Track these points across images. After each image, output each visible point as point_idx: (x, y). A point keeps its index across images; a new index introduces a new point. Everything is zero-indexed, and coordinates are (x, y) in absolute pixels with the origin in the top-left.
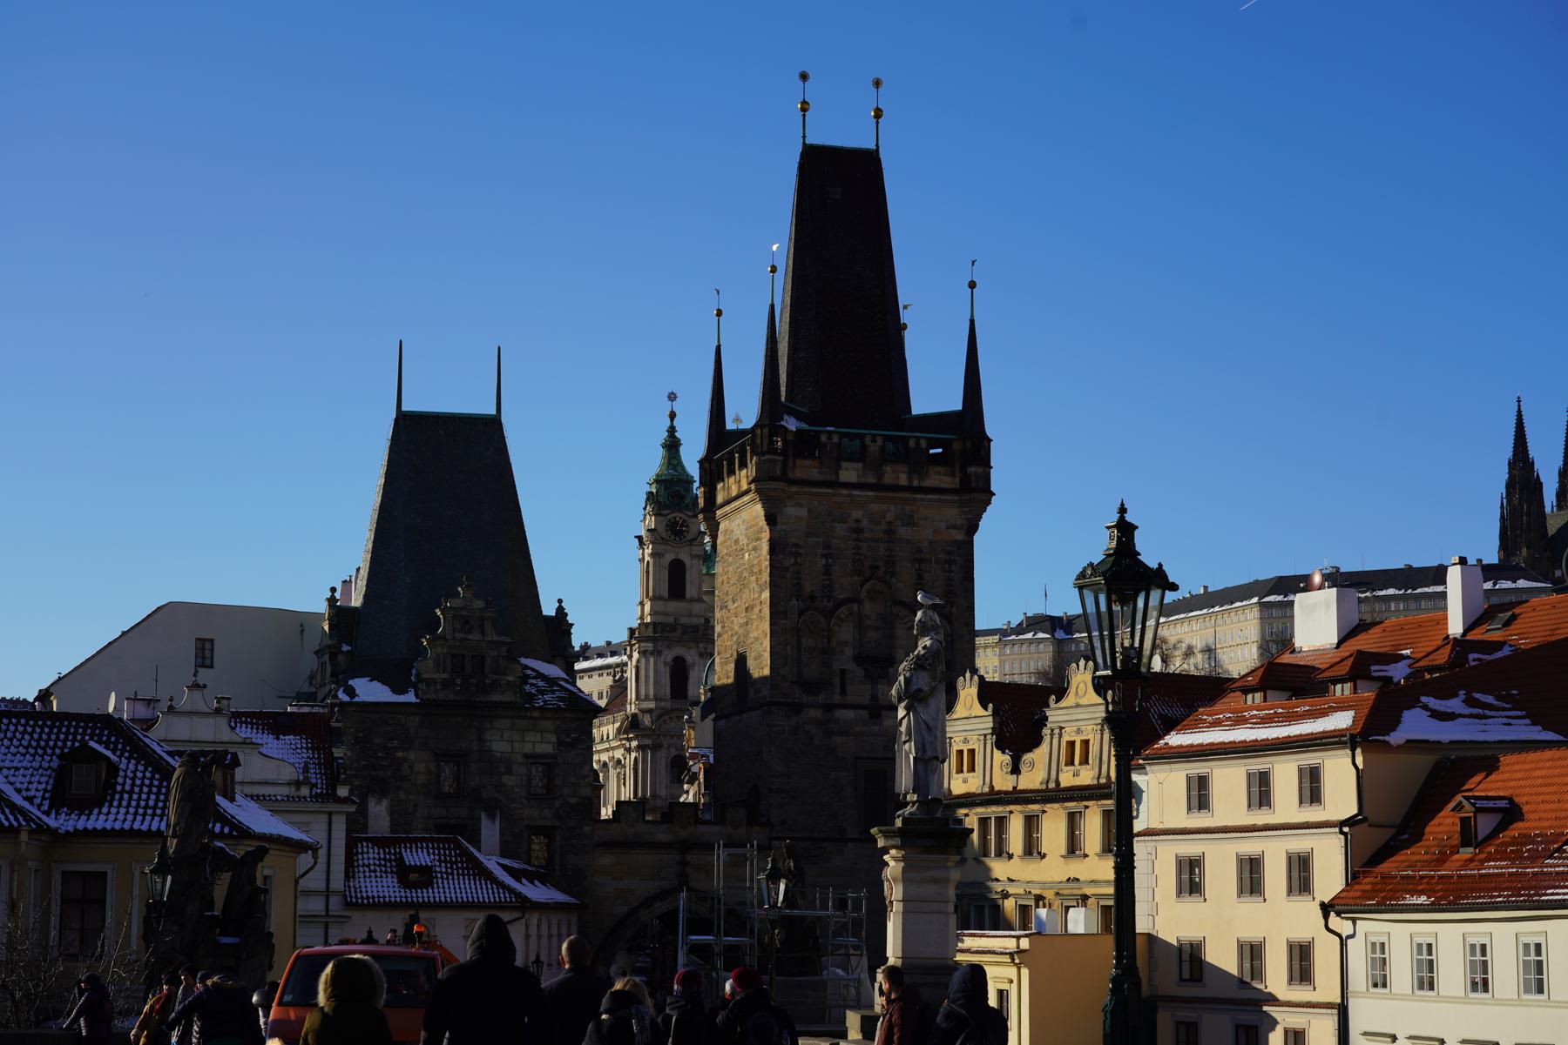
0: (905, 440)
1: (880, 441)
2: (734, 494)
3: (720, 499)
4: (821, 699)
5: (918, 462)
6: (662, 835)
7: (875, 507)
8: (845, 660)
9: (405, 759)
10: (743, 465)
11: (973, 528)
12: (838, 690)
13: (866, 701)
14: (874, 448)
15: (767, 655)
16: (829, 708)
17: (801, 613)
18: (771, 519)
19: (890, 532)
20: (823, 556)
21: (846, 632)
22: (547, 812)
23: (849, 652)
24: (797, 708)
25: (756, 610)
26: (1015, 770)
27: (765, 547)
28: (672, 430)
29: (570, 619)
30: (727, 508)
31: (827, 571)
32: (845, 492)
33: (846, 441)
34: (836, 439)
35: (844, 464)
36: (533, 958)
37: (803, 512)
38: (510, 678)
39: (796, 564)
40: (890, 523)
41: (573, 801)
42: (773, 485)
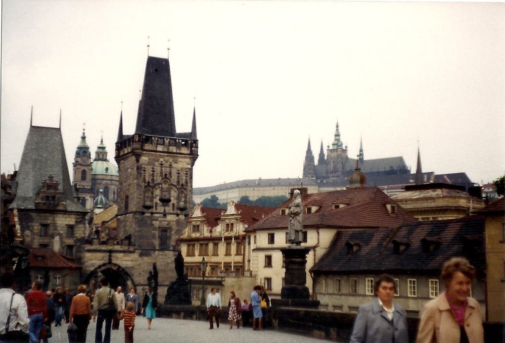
0: (176, 139)
2: (126, 152)
3: (121, 154)
4: (150, 210)
5: (177, 145)
7: (166, 158)
8: (157, 200)
9: (31, 225)
10: (129, 145)
11: (193, 165)
12: (154, 208)
13: (162, 211)
14: (167, 141)
19: (171, 166)
23: (158, 198)
24: (143, 213)
26: (211, 231)
27: (136, 168)
28: (84, 134)
32: (159, 153)
33: (159, 139)
35: (158, 146)
38: (64, 203)
40: (171, 163)
42: (138, 151)
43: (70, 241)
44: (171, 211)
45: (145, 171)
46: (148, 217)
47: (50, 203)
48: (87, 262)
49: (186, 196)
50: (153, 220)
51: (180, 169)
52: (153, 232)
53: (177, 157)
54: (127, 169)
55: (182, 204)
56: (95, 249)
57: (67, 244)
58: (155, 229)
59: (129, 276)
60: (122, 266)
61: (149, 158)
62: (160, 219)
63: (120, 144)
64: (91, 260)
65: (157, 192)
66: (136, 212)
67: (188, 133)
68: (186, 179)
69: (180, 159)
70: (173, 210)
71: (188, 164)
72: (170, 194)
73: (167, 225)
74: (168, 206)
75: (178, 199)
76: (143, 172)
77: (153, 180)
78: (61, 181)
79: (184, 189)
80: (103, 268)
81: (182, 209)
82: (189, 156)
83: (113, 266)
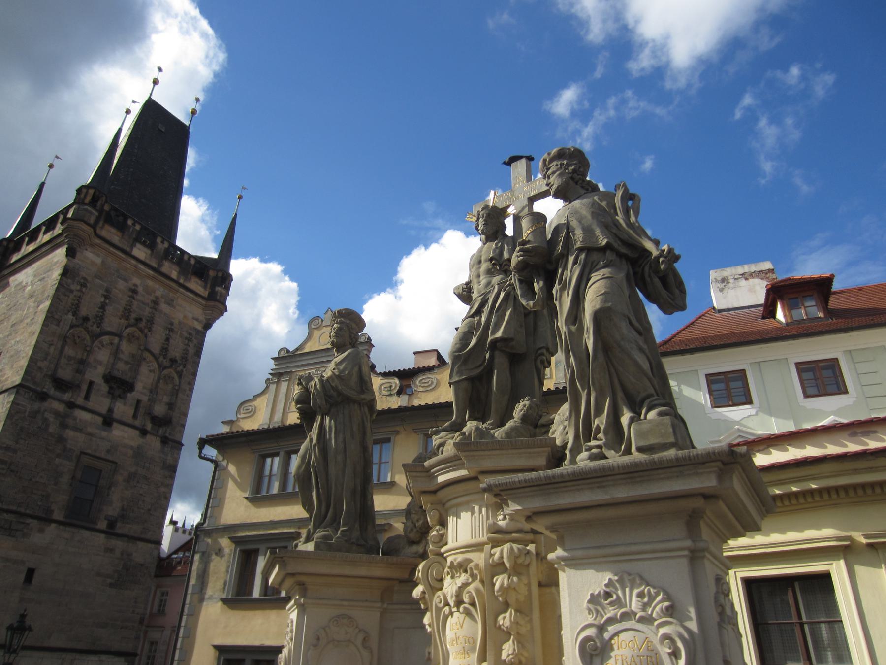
1: (166, 245)
4: (67, 396)
7: (150, 283)
8: (96, 374)
11: (208, 326)
12: (83, 394)
13: (104, 410)
14: (162, 246)
16: (71, 405)
17: (72, 327)
18: (71, 253)
19: (156, 303)
20: (103, 295)
21: (103, 355)
23: (101, 370)
24: (43, 397)
25: (28, 320)
30: (18, 265)
31: (103, 307)
32: (133, 262)
34: (138, 227)
35: (138, 245)
37: (98, 260)
39: (80, 291)
40: (157, 298)
44: (130, 421)
46: (57, 414)
49: (175, 392)
50: (64, 426)
51: (176, 322)
52: (57, 461)
53: (178, 291)
55: (159, 410)
61: (103, 262)
62: (89, 430)
65: (103, 355)
68: (186, 351)
70: (135, 416)
71: (197, 320)
72: (136, 371)
73: (108, 451)
74: (122, 397)
75: (153, 390)
76: (79, 287)
77: (102, 318)
79: (177, 372)
82: (204, 302)
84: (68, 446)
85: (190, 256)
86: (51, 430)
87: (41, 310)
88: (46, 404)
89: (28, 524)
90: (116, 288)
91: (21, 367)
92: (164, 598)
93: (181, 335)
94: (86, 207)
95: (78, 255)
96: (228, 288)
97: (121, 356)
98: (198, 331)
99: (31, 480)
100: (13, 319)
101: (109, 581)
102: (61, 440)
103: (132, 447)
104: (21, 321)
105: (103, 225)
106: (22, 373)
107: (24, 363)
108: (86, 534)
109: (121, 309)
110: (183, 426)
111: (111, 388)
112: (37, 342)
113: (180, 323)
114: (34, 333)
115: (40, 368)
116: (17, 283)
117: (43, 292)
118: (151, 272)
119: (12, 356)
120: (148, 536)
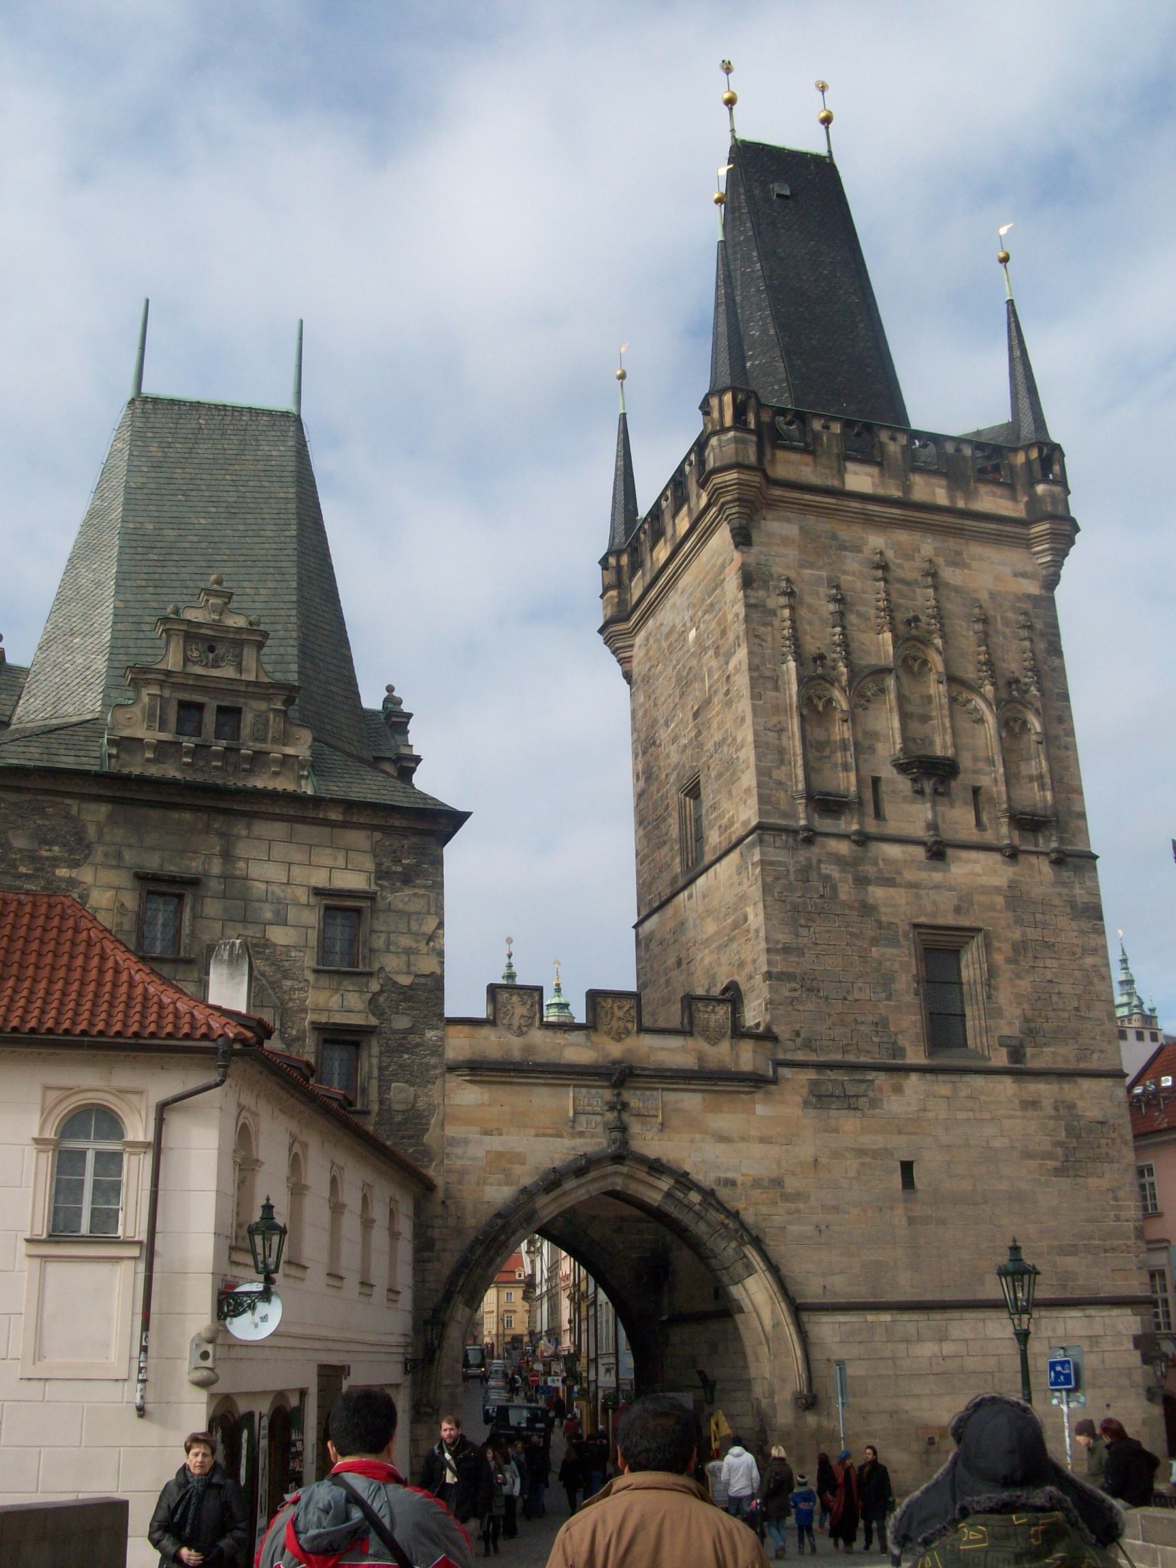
1: (903, 439)
6: (577, 1051)
7: (903, 536)
11: (1052, 581)
12: (870, 808)
13: (918, 830)
15: (748, 754)
18: (742, 538)
22: (355, 1000)
28: (510, 966)
29: (405, 708)
34: (836, 428)
35: (850, 466)
36: (257, 1216)
38: (290, 751)
41: (405, 980)
43: (345, 1005)
44: (973, 835)
45: (791, 594)
46: (839, 860)
47: (202, 748)
48: (466, 1141)
50: (862, 882)
51: (984, 596)
54: (684, 633)
56: (517, 1055)
57: (323, 1018)
58: (886, 934)
59: (757, 1242)
60: (697, 1176)
61: (801, 528)
62: (909, 875)
63: (625, 560)
64: (487, 1133)
66: (760, 827)
67: (1001, 426)
69: (976, 549)
70: (979, 823)
71: (1024, 575)
73: (958, 910)
76: (783, 600)
78: (295, 651)
80: (576, 1192)
81: (1029, 823)
83: (642, 1175)
84: (884, 919)
85: (959, 441)
86: (843, 896)
87: (737, 670)
88: (815, 850)
89: (872, 1081)
90: (845, 572)
91: (748, 790)
92: (1147, 1179)
93: (1006, 623)
94: (731, 434)
95: (755, 536)
96: (1062, 482)
97: (910, 708)
98: (1035, 600)
99: (845, 999)
100: (692, 703)
101: (1051, 1164)
102: (867, 909)
103: (998, 890)
104: (708, 702)
105: (773, 455)
106: (753, 801)
107: (749, 779)
108: (978, 1081)
109: (872, 612)
110: (1082, 816)
111: (914, 780)
112: (756, 734)
113: (993, 596)
114: (743, 719)
115: (780, 783)
116: (665, 630)
117: (724, 633)
118: (898, 511)
119: (720, 775)
120: (1094, 1064)
